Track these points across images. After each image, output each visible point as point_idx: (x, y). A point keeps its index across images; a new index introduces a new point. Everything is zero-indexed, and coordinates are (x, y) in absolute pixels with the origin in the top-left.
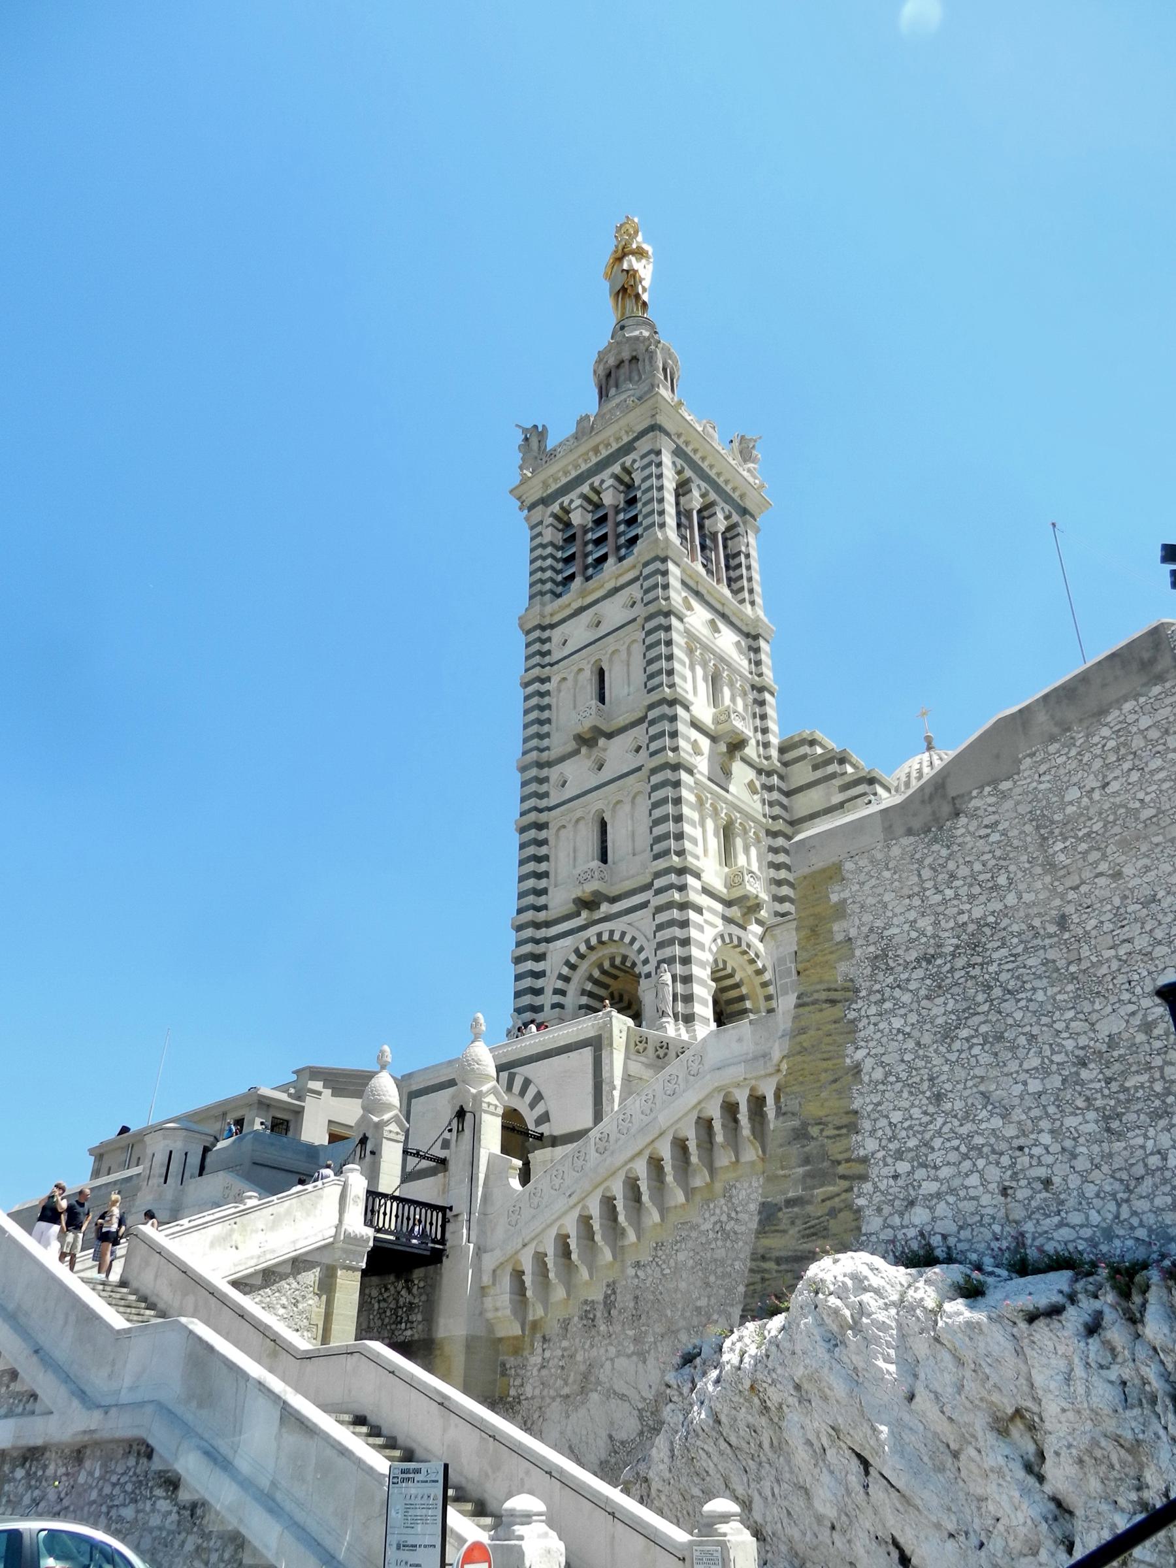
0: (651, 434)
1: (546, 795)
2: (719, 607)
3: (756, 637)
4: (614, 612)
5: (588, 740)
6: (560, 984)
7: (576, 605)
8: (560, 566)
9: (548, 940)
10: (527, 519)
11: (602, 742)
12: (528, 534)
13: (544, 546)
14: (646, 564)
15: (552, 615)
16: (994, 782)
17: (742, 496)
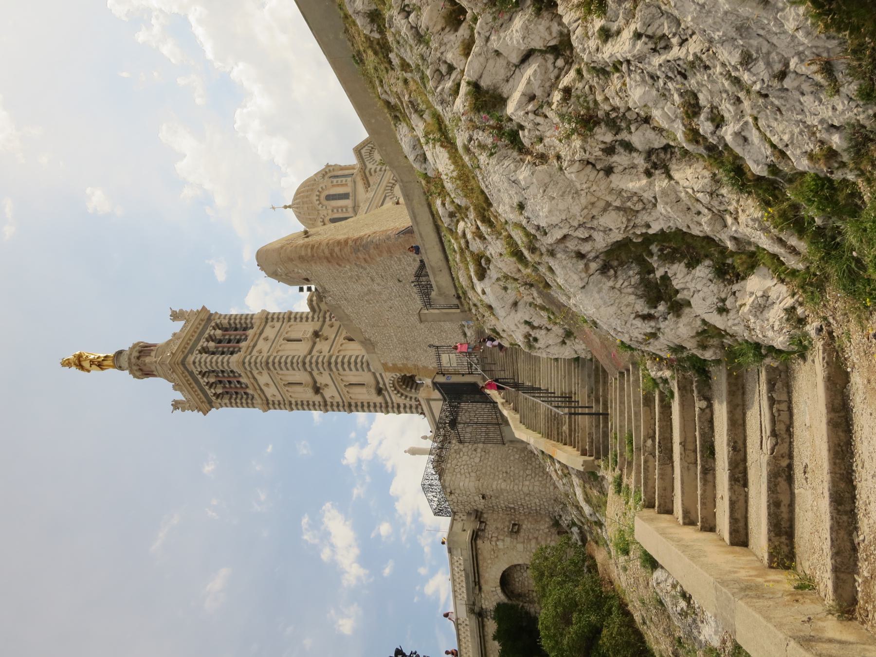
0: (187, 366)
1: (338, 403)
2: (257, 336)
3: (267, 319)
4: (264, 379)
5: (317, 390)
6: (408, 399)
7: (259, 392)
8: (239, 396)
9: (392, 403)
10: (217, 408)
11: (318, 385)
12: (224, 410)
13: (231, 403)
14: (245, 369)
15: (262, 400)
16: (362, 332)
17: (202, 320)
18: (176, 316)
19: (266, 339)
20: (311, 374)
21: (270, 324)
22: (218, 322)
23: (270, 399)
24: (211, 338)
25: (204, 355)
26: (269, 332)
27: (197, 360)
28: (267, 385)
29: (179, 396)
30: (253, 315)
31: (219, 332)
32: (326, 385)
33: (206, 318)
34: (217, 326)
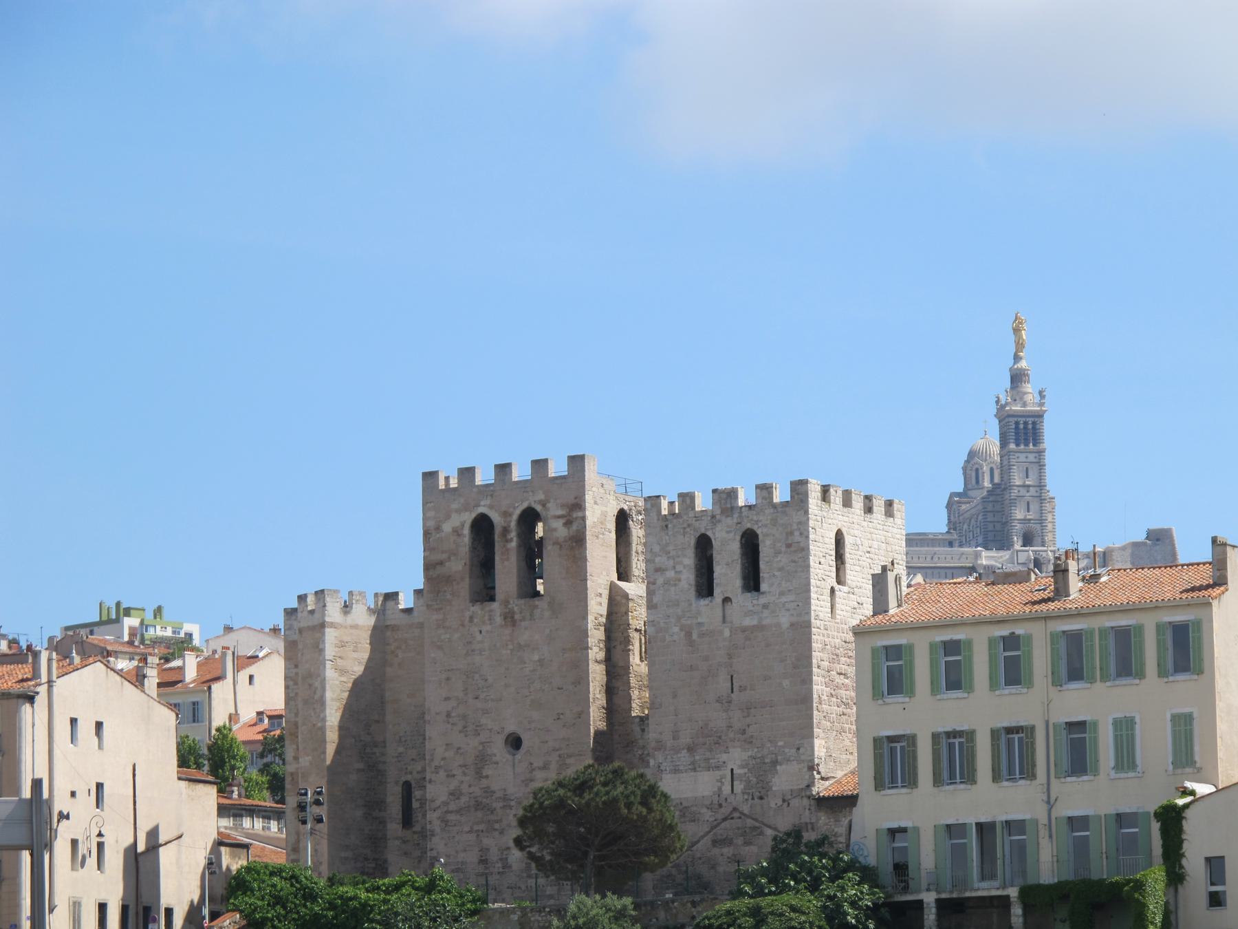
18: (1041, 394)
19: (1027, 457)
21: (1037, 455)
24: (1026, 423)
25: (1013, 427)
26: (1032, 457)
27: (1010, 424)
33: (1040, 416)
34: (1034, 423)
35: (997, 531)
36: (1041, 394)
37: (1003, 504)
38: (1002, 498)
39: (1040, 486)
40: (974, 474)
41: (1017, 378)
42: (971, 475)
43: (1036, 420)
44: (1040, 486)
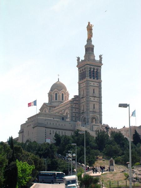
3: (100, 82)
5: (82, 98)
18: (100, 57)
20: (85, 97)
21: (98, 83)
22: (99, 69)
23: (81, 84)
24: (94, 69)
25: (89, 69)
26: (96, 84)
27: (88, 68)
28: (83, 85)
29: (80, 61)
30: (101, 78)
31: (96, 70)
32: (83, 100)
35: (76, 117)
36: (100, 57)
37: (80, 105)
38: (80, 102)
39: (100, 98)
40: (55, 96)
41: (89, 49)
42: (53, 96)
43: (98, 68)
44: (100, 98)
